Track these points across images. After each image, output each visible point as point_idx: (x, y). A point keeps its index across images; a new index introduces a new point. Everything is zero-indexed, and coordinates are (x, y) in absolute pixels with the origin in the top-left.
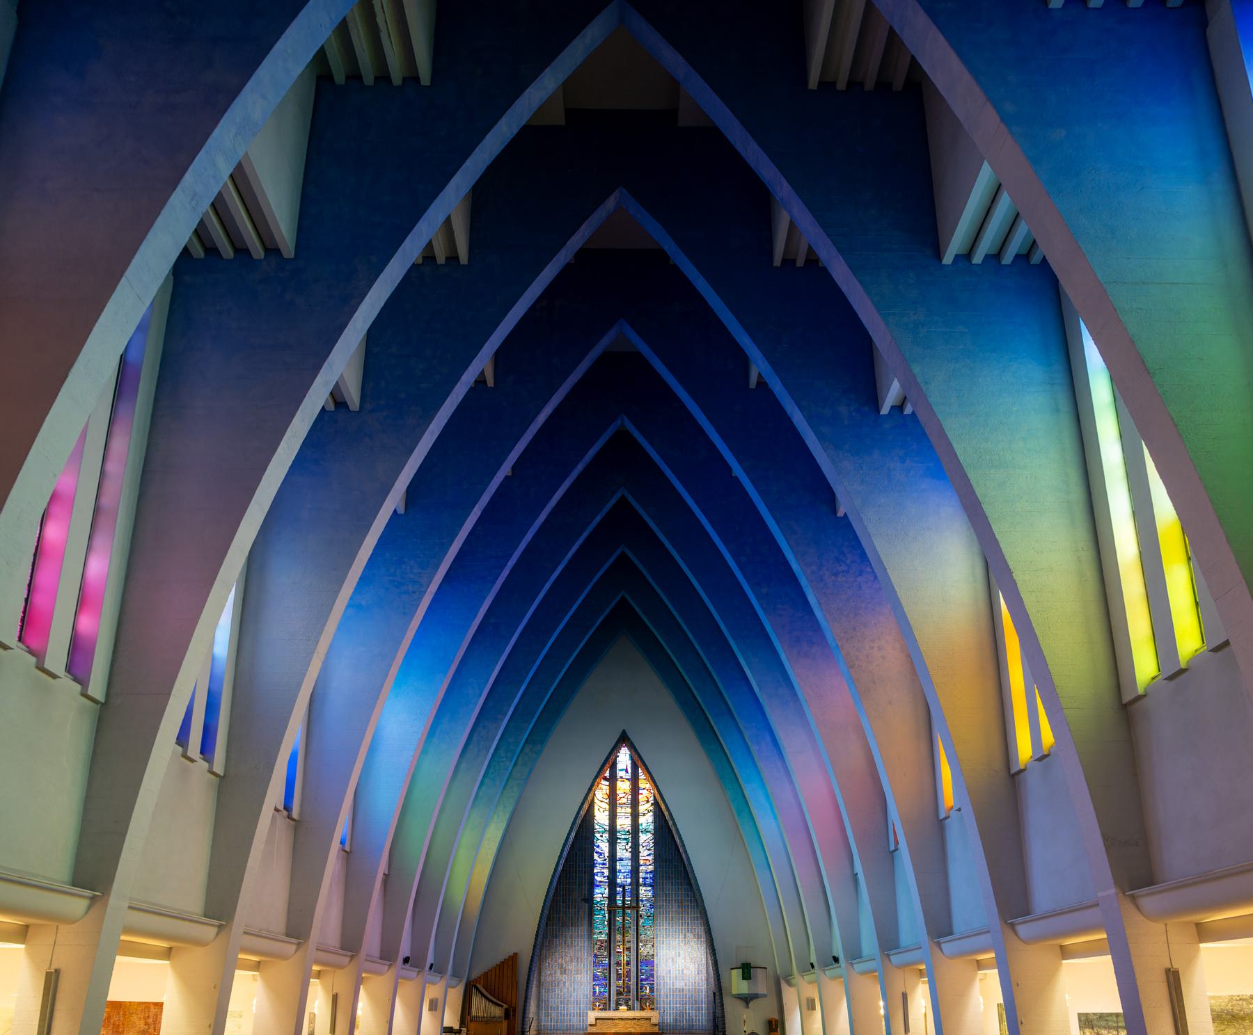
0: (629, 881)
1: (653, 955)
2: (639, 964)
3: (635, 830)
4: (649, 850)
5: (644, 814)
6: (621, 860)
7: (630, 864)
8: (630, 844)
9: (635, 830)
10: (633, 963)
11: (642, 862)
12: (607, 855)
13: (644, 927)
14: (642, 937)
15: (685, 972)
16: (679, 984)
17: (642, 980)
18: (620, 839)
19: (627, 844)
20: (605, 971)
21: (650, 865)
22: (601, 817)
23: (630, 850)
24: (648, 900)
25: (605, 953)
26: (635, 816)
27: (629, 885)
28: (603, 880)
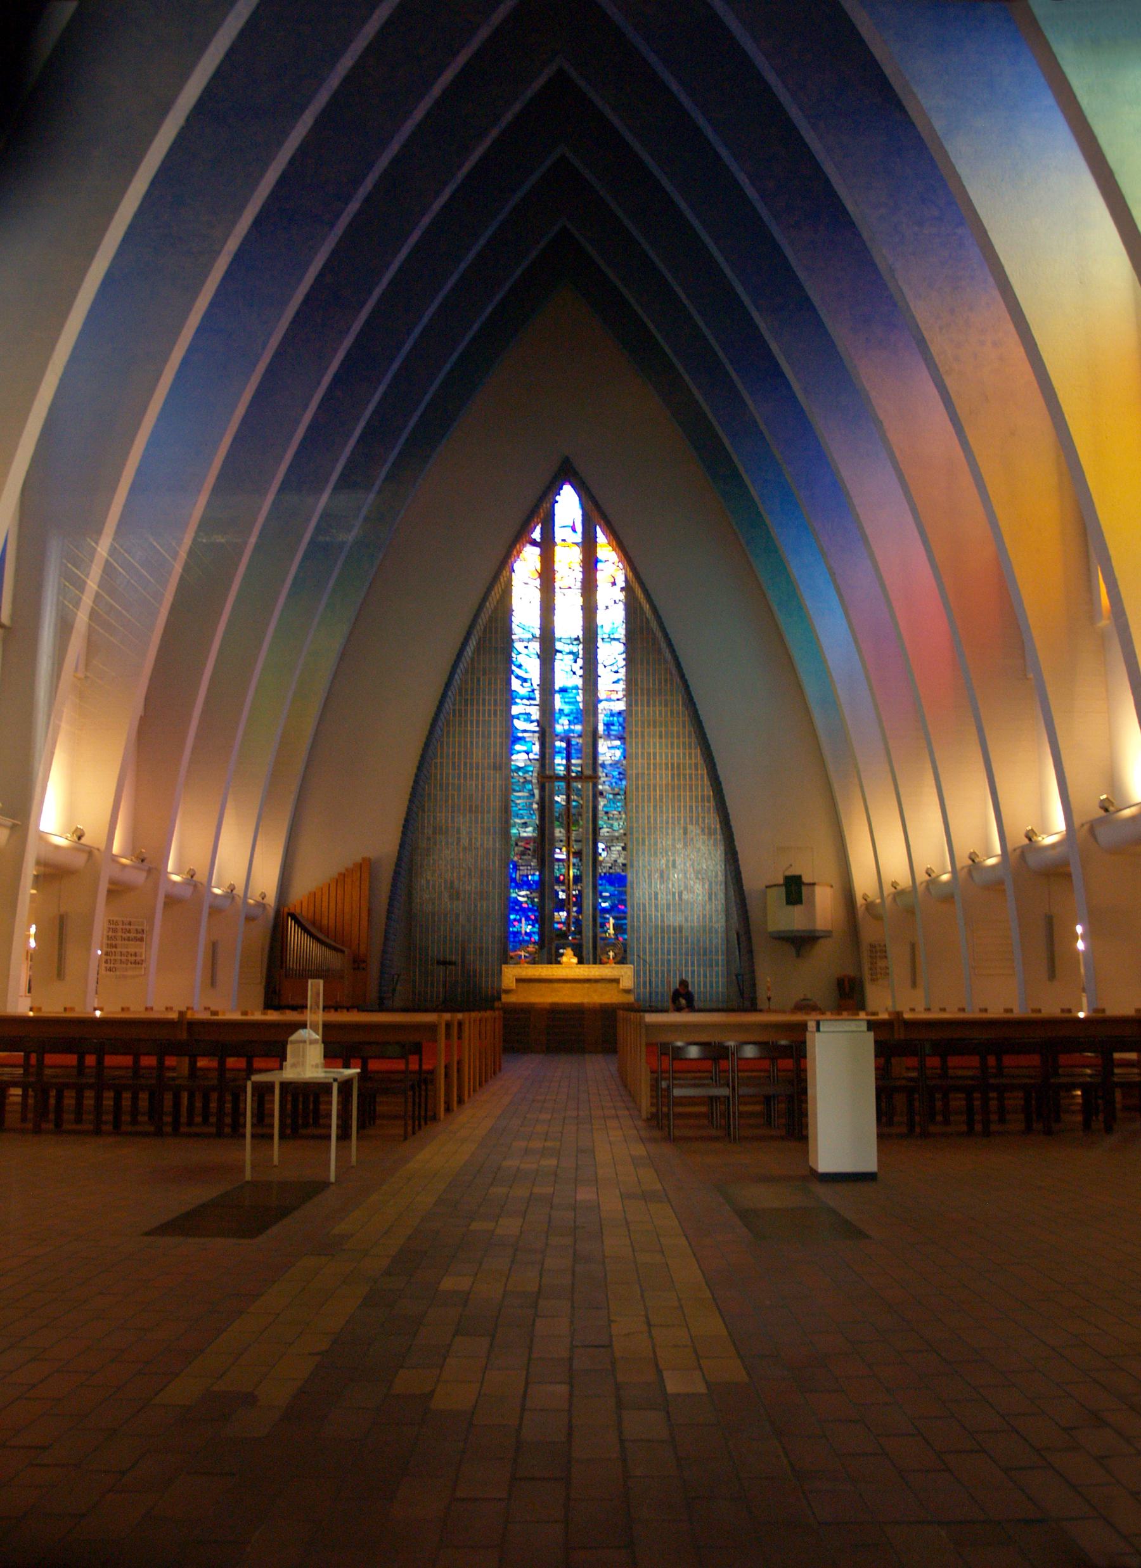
12: (536, 681)
13: (607, 813)
15: (685, 896)
16: (675, 919)
18: (561, 652)
24: (615, 764)
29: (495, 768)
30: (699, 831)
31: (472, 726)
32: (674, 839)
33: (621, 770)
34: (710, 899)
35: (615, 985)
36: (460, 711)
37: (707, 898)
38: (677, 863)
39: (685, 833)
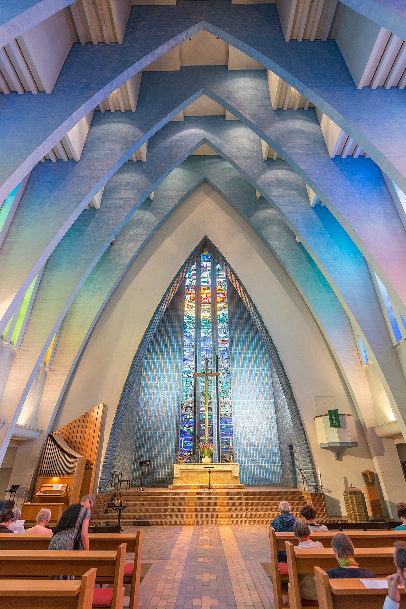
1: (231, 413)
2: (220, 422)
3: (214, 321)
5: (221, 310)
8: (211, 329)
9: (214, 321)
13: (223, 390)
14: (221, 399)
15: (259, 428)
16: (255, 439)
17: (222, 435)
19: (209, 330)
20: (191, 428)
22: (189, 311)
24: (226, 370)
25: (191, 413)
26: (214, 311)
28: (190, 355)
29: (176, 372)
30: (263, 398)
31: (167, 355)
33: (228, 372)
34: (270, 429)
35: (230, 474)
36: (162, 349)
37: (269, 429)
38: (255, 412)
39: (257, 399)
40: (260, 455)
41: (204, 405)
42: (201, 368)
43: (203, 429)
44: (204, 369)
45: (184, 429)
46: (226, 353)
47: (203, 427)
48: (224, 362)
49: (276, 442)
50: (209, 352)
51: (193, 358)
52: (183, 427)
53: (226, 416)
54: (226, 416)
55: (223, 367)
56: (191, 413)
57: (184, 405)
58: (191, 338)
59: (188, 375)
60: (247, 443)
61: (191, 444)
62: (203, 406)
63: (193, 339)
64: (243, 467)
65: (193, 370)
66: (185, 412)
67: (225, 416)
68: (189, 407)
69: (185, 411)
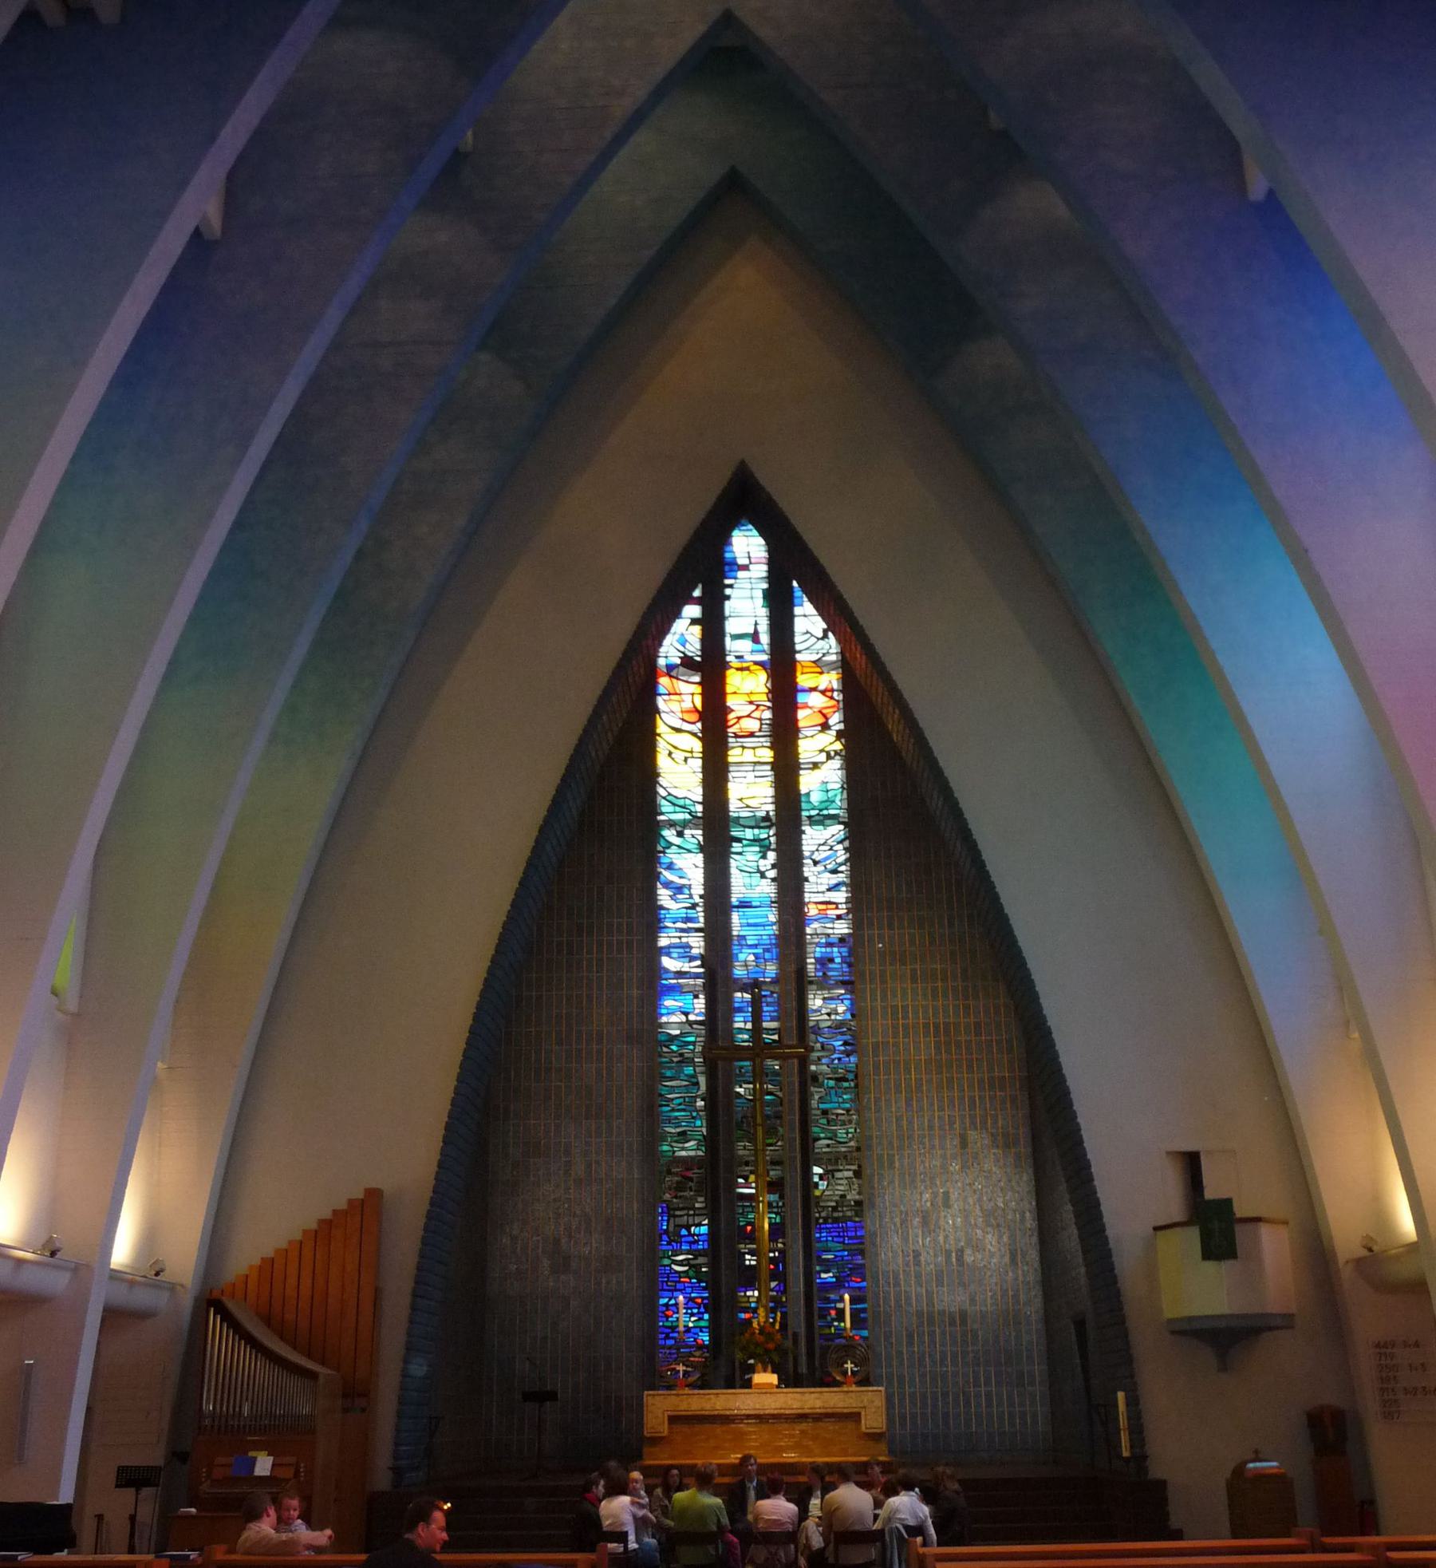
0: (771, 970)
4: (834, 872)
5: (815, 766)
6: (745, 905)
7: (773, 918)
8: (772, 856)
10: (796, 1232)
11: (812, 911)
12: (698, 890)
13: (825, 1112)
15: (969, 1257)
16: (950, 1299)
19: (764, 857)
20: (701, 1260)
21: (839, 917)
23: (772, 874)
26: (786, 769)
27: (775, 981)
32: (944, 1157)
33: (847, 1037)
37: (1007, 1259)
39: (964, 1144)
40: (971, 1355)
41: (752, 1172)
42: (737, 1025)
43: (747, 1263)
44: (749, 1026)
45: (673, 1266)
46: (838, 960)
47: (748, 1257)
48: (832, 999)
49: (1033, 1309)
50: (767, 955)
51: (700, 981)
52: (669, 1257)
53: (841, 1214)
54: (841, 1214)
55: (826, 1017)
56: (697, 1205)
57: (669, 1172)
58: (691, 897)
59: (681, 1055)
60: (920, 1314)
61: (701, 1319)
62: (746, 1178)
63: (697, 899)
64: (902, 1400)
65: (703, 1032)
66: (675, 1200)
67: (836, 1215)
68: (691, 1179)
69: (676, 1197)
